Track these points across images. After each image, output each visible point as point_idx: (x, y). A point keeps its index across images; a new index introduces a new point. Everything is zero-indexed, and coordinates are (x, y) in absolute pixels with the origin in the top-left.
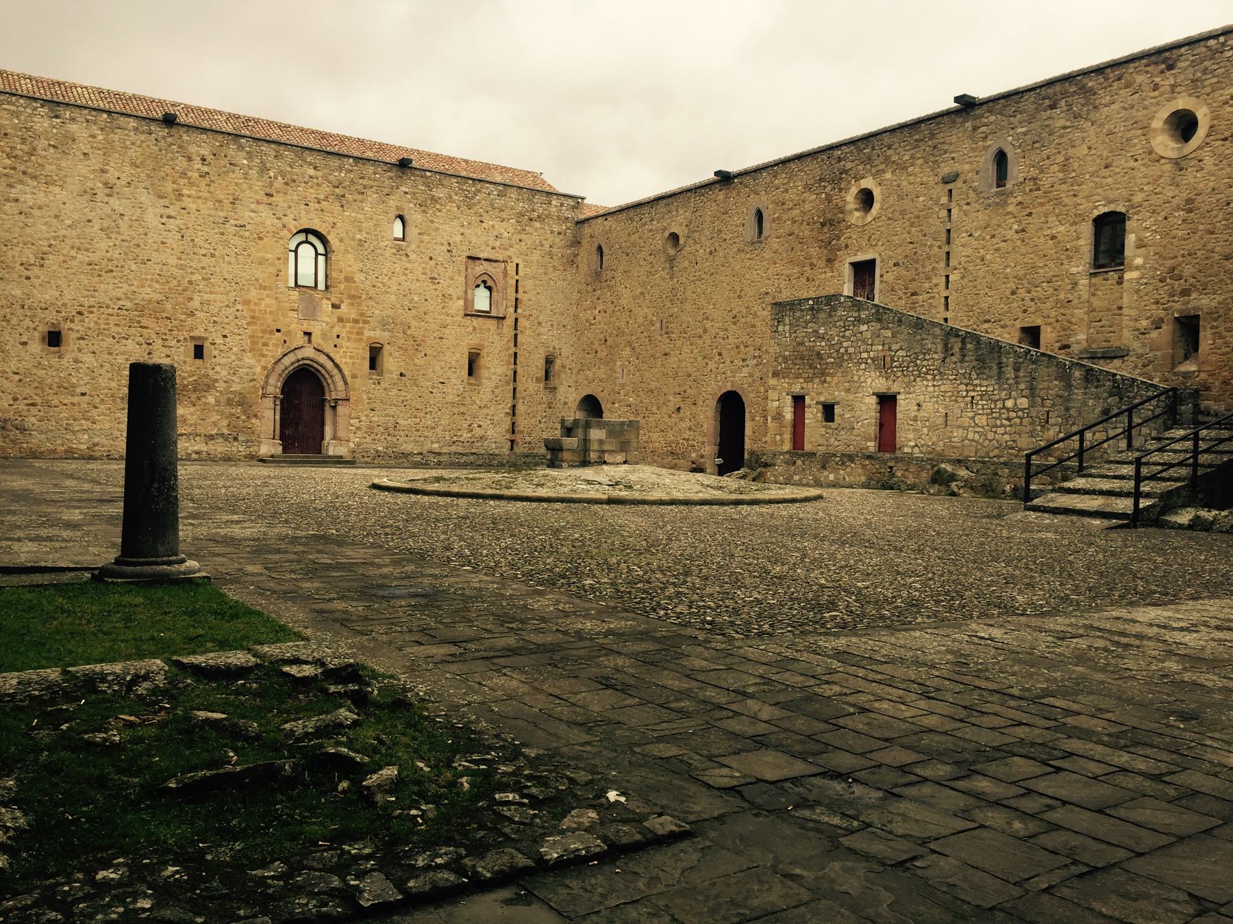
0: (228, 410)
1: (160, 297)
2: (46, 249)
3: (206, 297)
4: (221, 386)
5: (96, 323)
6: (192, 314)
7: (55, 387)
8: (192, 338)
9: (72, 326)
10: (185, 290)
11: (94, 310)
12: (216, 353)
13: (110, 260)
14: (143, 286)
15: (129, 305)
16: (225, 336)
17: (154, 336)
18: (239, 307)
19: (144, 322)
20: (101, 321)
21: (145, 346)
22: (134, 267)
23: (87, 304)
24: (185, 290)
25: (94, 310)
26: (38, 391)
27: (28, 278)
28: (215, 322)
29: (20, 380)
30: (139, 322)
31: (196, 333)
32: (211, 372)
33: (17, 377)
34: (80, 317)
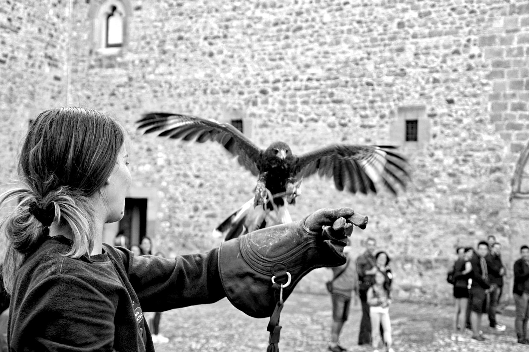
0: (455, 220)
1: (360, 54)
2: (229, 14)
3: (423, 42)
4: (443, 181)
5: (282, 103)
6: (403, 74)
7: (235, 192)
8: (401, 110)
9: (254, 110)
10: (392, 39)
11: (279, 85)
12: (436, 129)
13: (299, 14)
14: (338, 43)
15: (320, 72)
16: (451, 102)
17: (349, 112)
18: (474, 50)
19: (339, 93)
20: (287, 100)
21: (338, 128)
22: (327, 18)
23: (271, 79)
24: (392, 39)
25: (279, 85)
26: (219, 198)
27: (211, 55)
28: (436, 81)
29: (201, 185)
30: (332, 95)
31: (407, 102)
32: (428, 161)
33: (198, 182)
34: (263, 97)
